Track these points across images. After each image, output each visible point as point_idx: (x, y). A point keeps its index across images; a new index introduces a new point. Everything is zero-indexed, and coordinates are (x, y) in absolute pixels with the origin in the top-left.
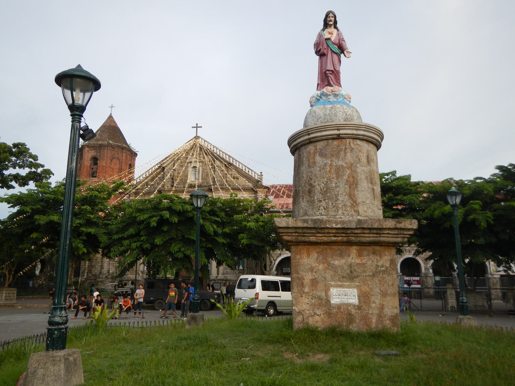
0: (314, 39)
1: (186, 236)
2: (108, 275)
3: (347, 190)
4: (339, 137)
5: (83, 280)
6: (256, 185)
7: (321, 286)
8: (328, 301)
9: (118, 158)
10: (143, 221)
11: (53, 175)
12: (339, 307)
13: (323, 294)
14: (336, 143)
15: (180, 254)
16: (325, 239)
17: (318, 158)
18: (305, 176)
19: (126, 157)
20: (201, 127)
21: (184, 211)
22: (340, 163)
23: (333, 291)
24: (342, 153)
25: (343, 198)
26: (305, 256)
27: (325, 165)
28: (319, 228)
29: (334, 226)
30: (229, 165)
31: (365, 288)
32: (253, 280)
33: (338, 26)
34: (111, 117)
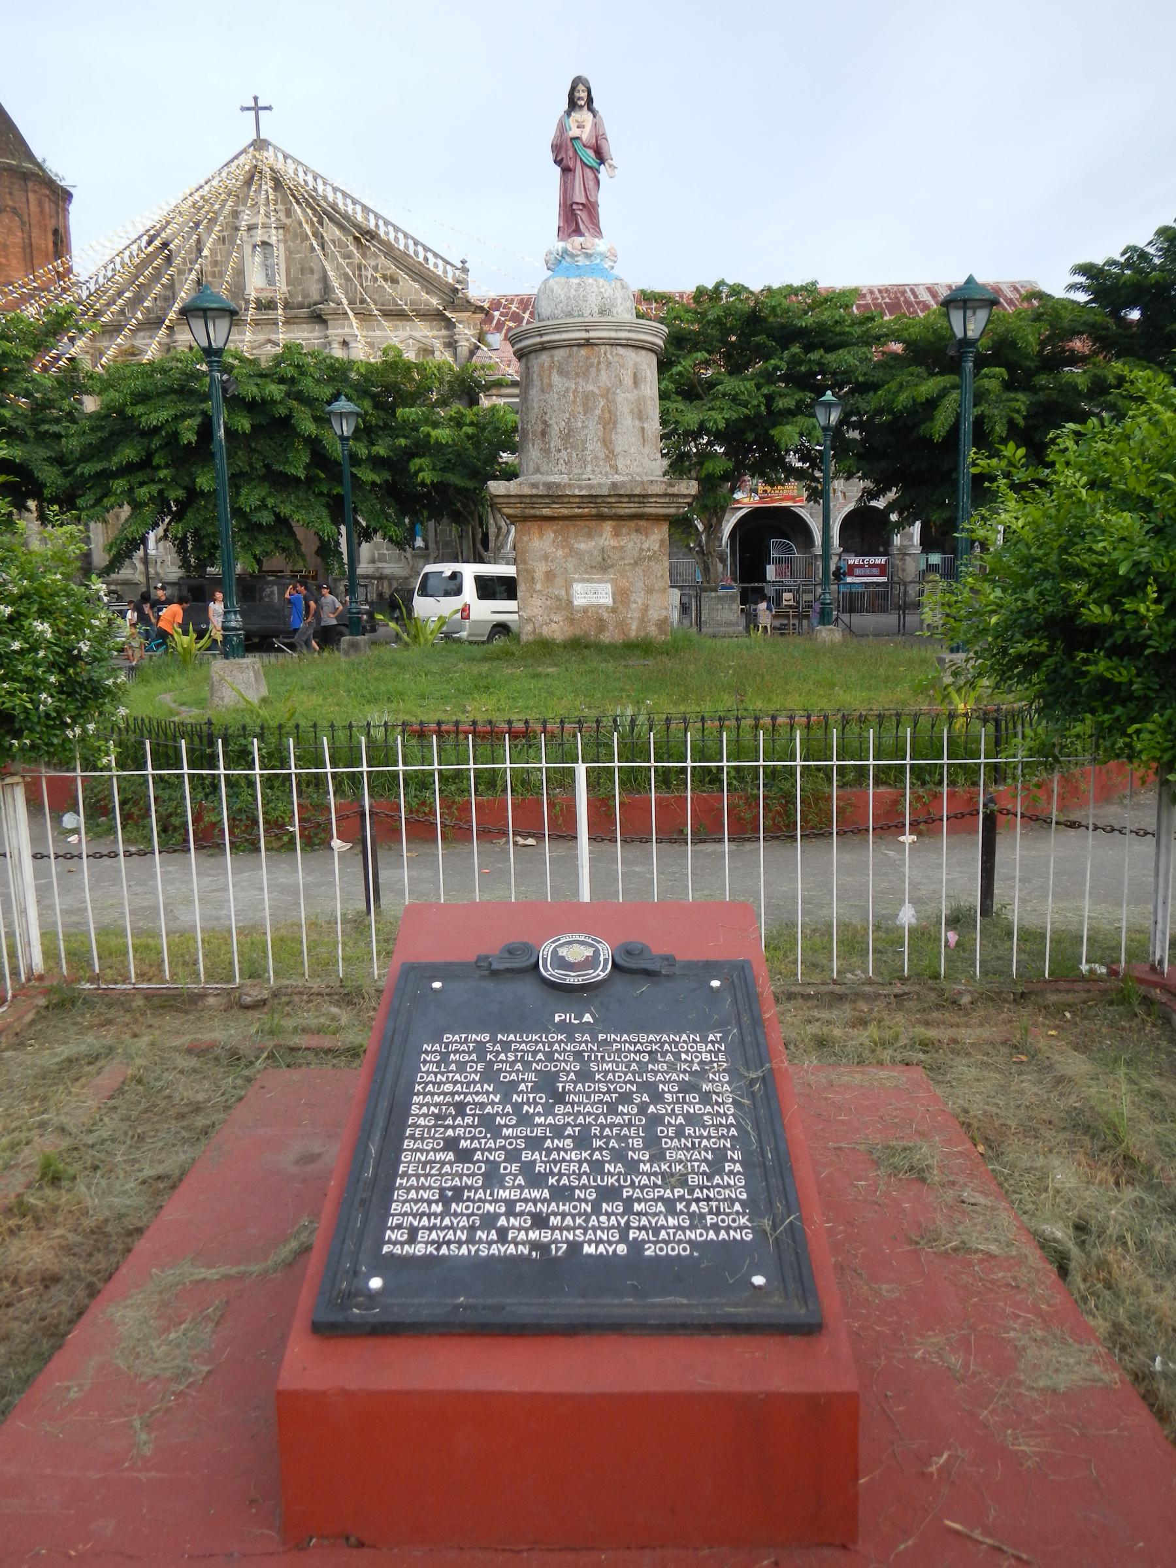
0: (549, 135)
1: (275, 467)
3: (600, 433)
4: (588, 343)
6: (450, 302)
7: (559, 581)
8: (570, 602)
9: (15, 211)
10: (156, 430)
12: (585, 610)
13: (563, 593)
14: (583, 352)
15: (265, 513)
16: (565, 512)
17: (556, 378)
18: (536, 406)
19: (40, 203)
20: (269, 108)
21: (263, 399)
22: (590, 387)
23: (578, 588)
24: (593, 370)
25: (594, 447)
26: (536, 537)
27: (567, 389)
28: (554, 496)
29: (577, 492)
30: (365, 237)
31: (623, 583)
32: (455, 576)
33: (596, 105)
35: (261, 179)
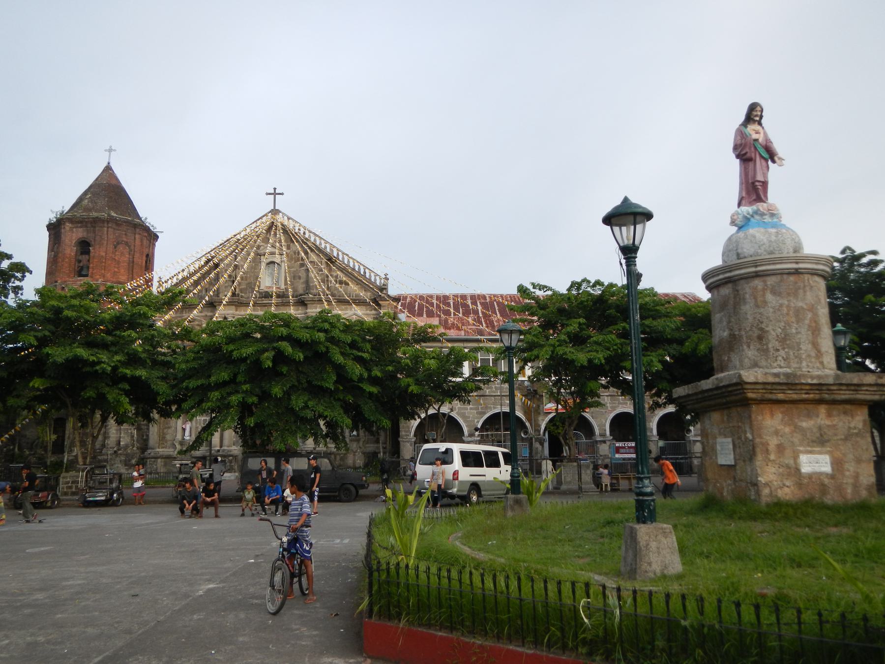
1: (315, 383)
2: (119, 450)
3: (810, 338)
4: (797, 272)
5: (70, 458)
6: (378, 295)
7: (788, 452)
8: (798, 470)
9: (127, 244)
10: (243, 360)
11: (31, 272)
12: (810, 476)
13: (792, 462)
14: (792, 278)
15: (308, 411)
16: (795, 397)
17: (769, 297)
18: (750, 318)
19: (142, 241)
21: (312, 340)
22: (800, 304)
23: (804, 458)
24: (801, 291)
25: (806, 347)
26: (768, 417)
27: (781, 305)
28: (791, 384)
29: (810, 381)
30: (331, 260)
31: (838, 454)
32: (448, 452)
33: (763, 121)
34: (108, 169)
35: (276, 230)
